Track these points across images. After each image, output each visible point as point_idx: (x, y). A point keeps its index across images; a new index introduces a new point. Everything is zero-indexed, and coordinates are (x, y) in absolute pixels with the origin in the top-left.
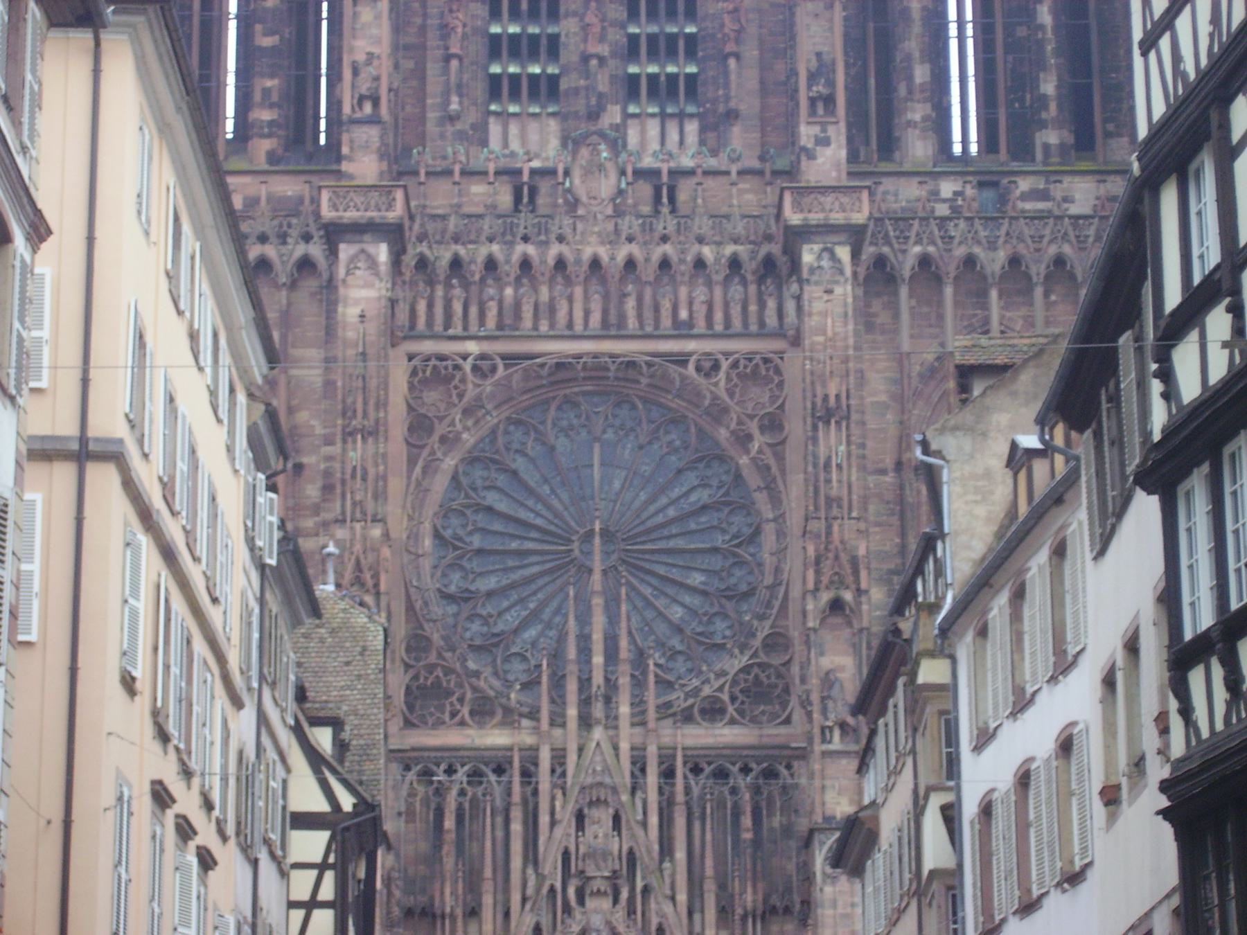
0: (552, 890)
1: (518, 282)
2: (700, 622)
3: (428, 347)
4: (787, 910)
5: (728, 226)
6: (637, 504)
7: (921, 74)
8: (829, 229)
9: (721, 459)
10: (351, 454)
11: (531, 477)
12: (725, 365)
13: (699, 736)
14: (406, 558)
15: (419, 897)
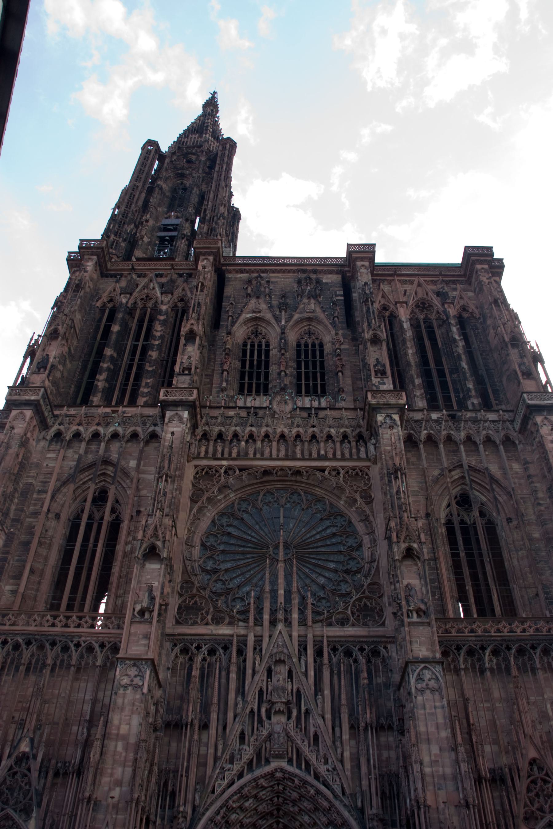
0: (252, 711)
1: (247, 442)
2: (334, 585)
3: (205, 462)
4: (390, 728)
5: (342, 422)
6: (301, 533)
7: (418, 381)
8: (389, 406)
9: (341, 515)
10: (160, 483)
11: (250, 521)
12: (342, 472)
13: (336, 631)
14: (185, 547)
15: (175, 716)
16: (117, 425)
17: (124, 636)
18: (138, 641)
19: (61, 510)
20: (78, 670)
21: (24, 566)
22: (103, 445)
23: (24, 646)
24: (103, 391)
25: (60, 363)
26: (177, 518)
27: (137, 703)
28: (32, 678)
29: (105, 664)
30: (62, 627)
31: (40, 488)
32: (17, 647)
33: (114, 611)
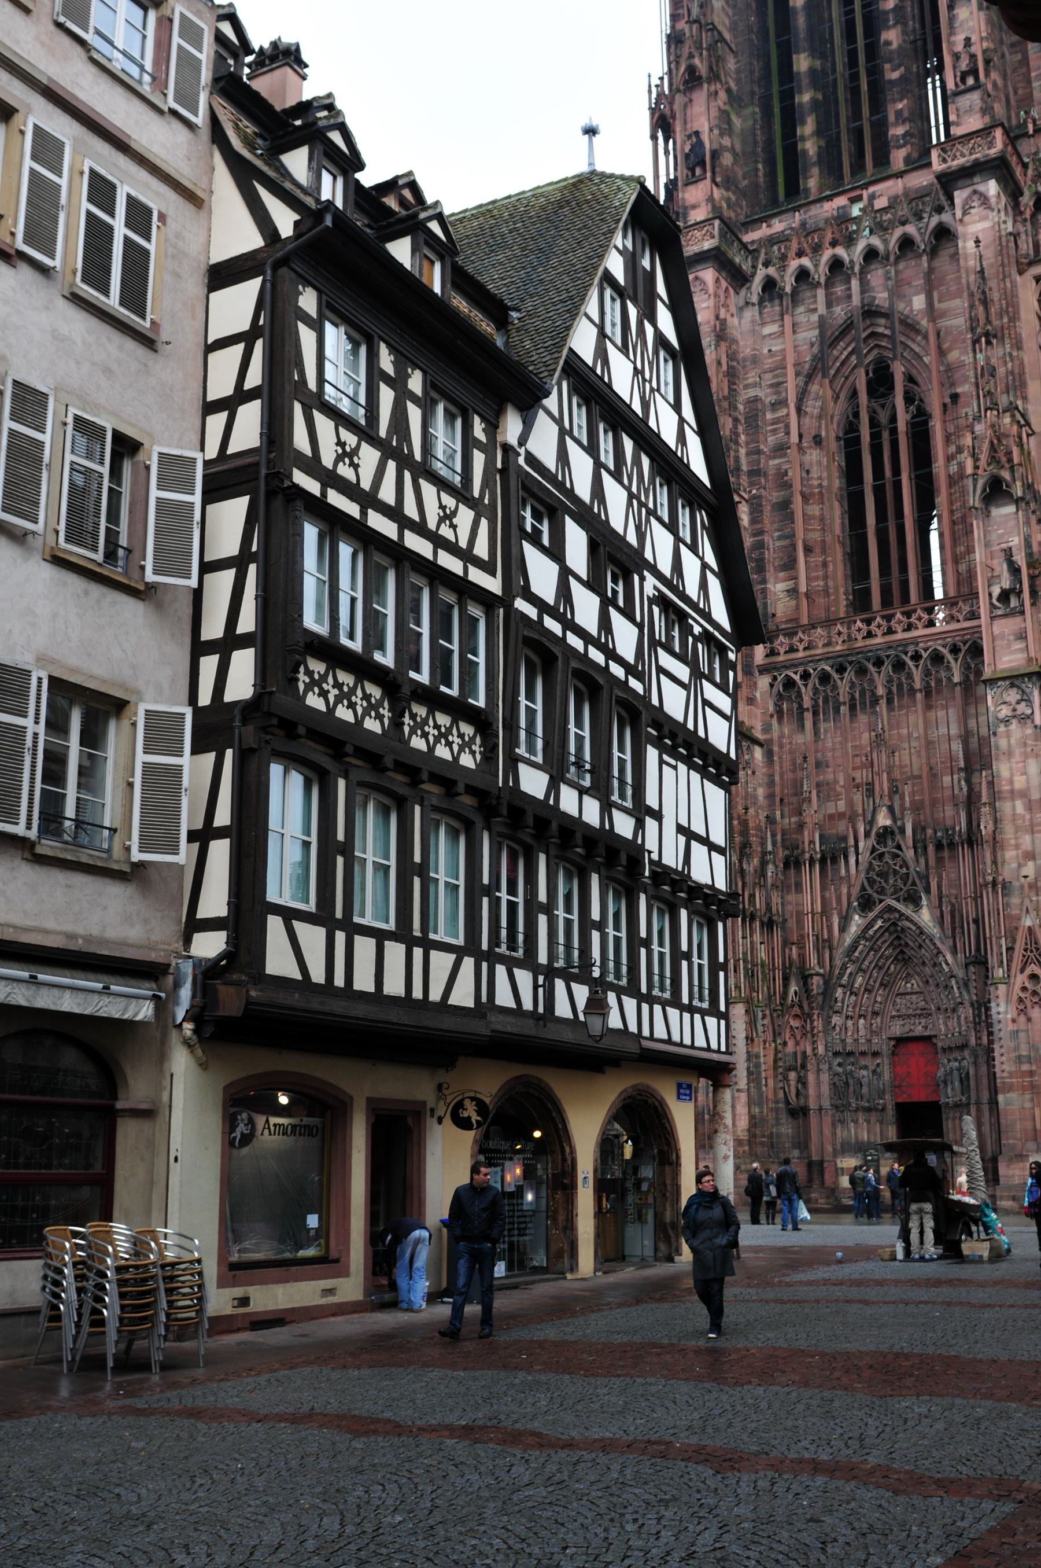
10: (978, 356)
16: (867, 232)
17: (983, 629)
18: (1009, 646)
19: (820, 427)
20: (928, 692)
21: (794, 546)
22: (855, 283)
23: (836, 676)
24: (820, 162)
25: (721, 135)
26: (1025, 398)
27: (1029, 742)
28: (863, 718)
29: (967, 677)
30: (884, 634)
31: (773, 398)
32: (825, 678)
33: (959, 590)
